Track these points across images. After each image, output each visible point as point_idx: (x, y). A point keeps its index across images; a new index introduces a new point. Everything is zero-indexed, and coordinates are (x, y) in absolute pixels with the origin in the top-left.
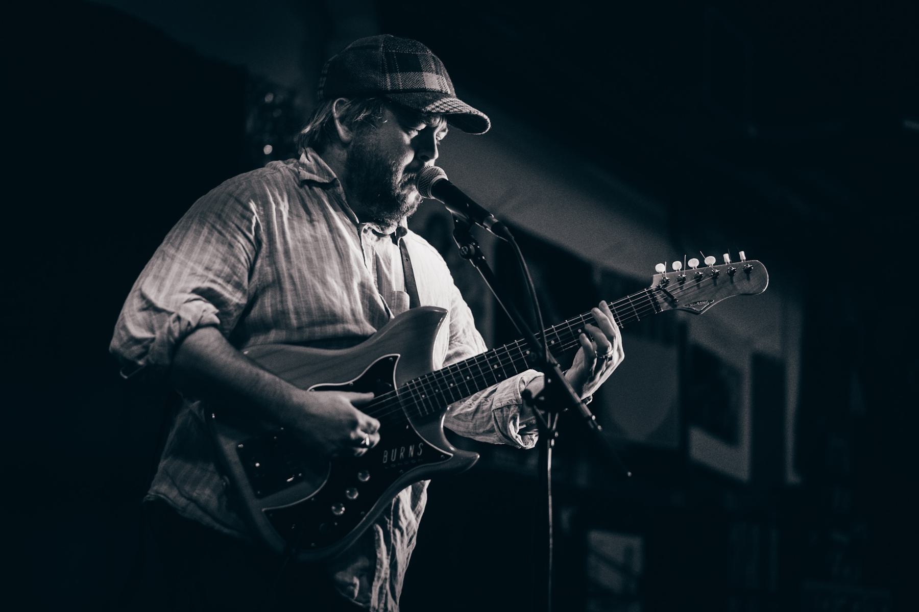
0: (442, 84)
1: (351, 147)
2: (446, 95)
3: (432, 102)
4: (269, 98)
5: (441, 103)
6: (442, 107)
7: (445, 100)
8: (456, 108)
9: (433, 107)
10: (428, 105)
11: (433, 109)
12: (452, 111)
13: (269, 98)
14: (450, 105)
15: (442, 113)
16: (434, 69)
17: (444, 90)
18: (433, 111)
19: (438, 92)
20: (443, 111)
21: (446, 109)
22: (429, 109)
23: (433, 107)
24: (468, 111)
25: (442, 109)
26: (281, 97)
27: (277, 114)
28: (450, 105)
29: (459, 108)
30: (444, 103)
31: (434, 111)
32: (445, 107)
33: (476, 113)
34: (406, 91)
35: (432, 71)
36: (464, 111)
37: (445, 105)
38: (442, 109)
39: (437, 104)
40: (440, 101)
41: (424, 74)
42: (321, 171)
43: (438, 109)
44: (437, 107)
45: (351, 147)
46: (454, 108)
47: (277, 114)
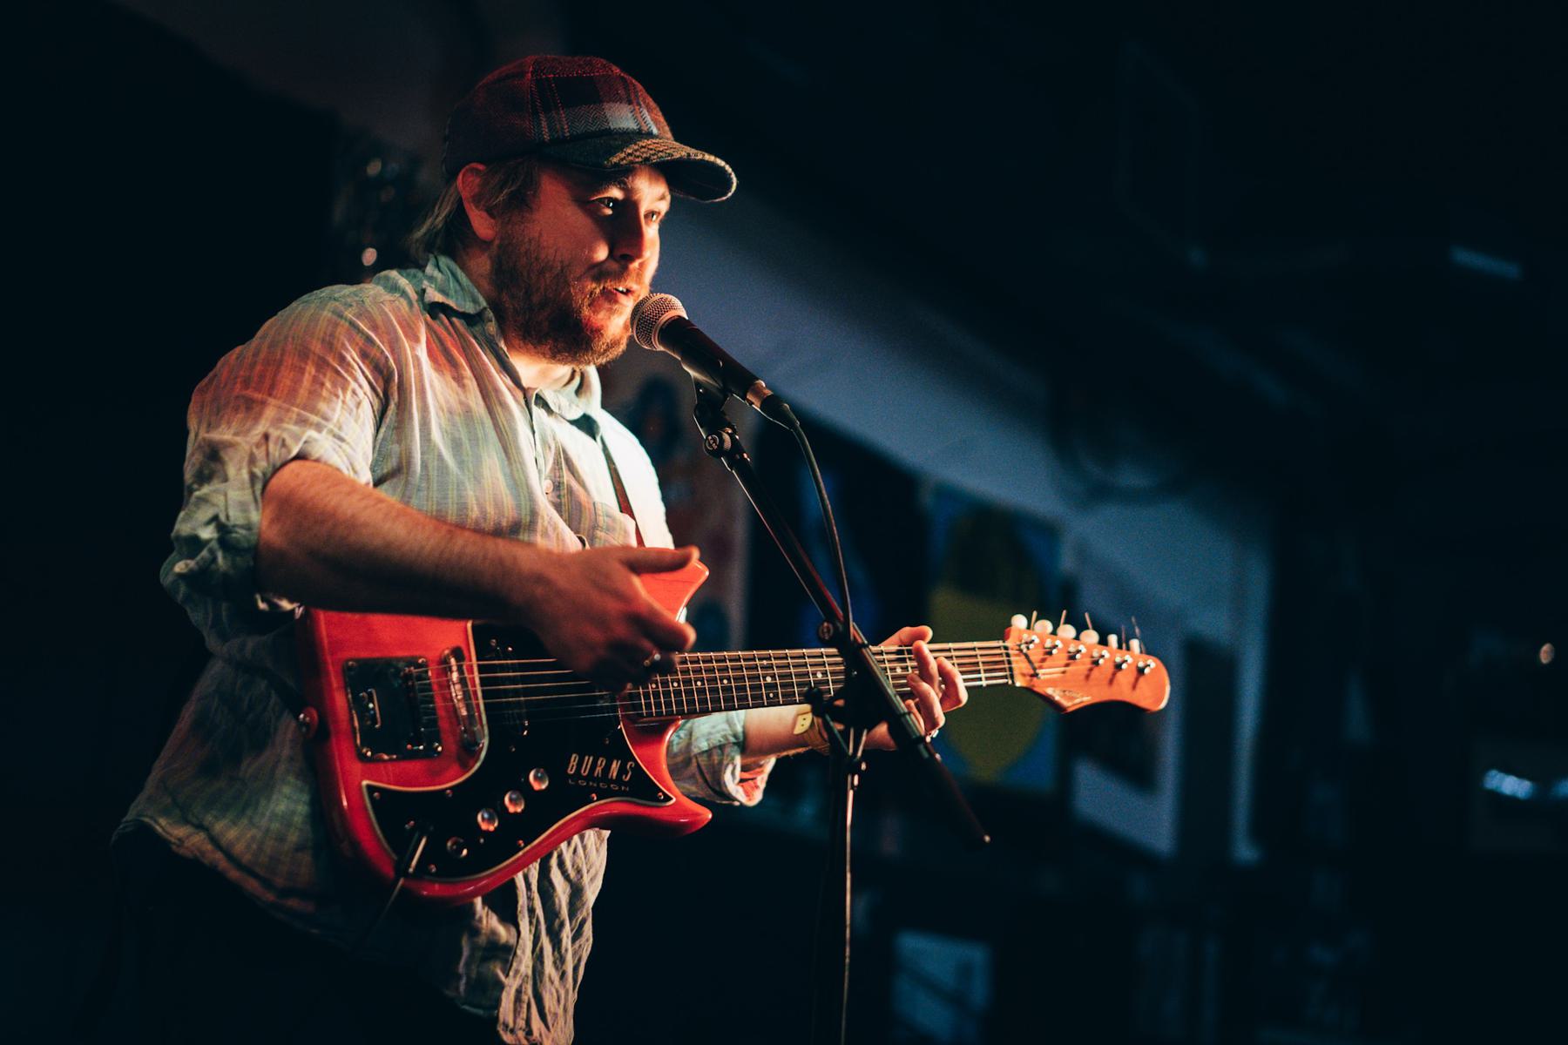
1: (494, 247)
4: (374, 168)
5: (636, 147)
6: (638, 153)
8: (662, 151)
9: (623, 155)
10: (613, 154)
11: (622, 159)
12: (655, 157)
13: (374, 168)
14: (651, 149)
18: (622, 163)
21: (645, 155)
22: (615, 160)
23: (623, 155)
24: (683, 153)
25: (638, 157)
26: (394, 166)
27: (387, 195)
28: (651, 149)
29: (668, 151)
30: (643, 147)
32: (643, 153)
33: (700, 157)
34: (575, 138)
36: (677, 156)
37: (643, 150)
38: (638, 157)
39: (630, 151)
40: (635, 144)
41: (606, 106)
42: (461, 293)
43: (630, 158)
45: (494, 247)
46: (659, 151)
47: (387, 195)
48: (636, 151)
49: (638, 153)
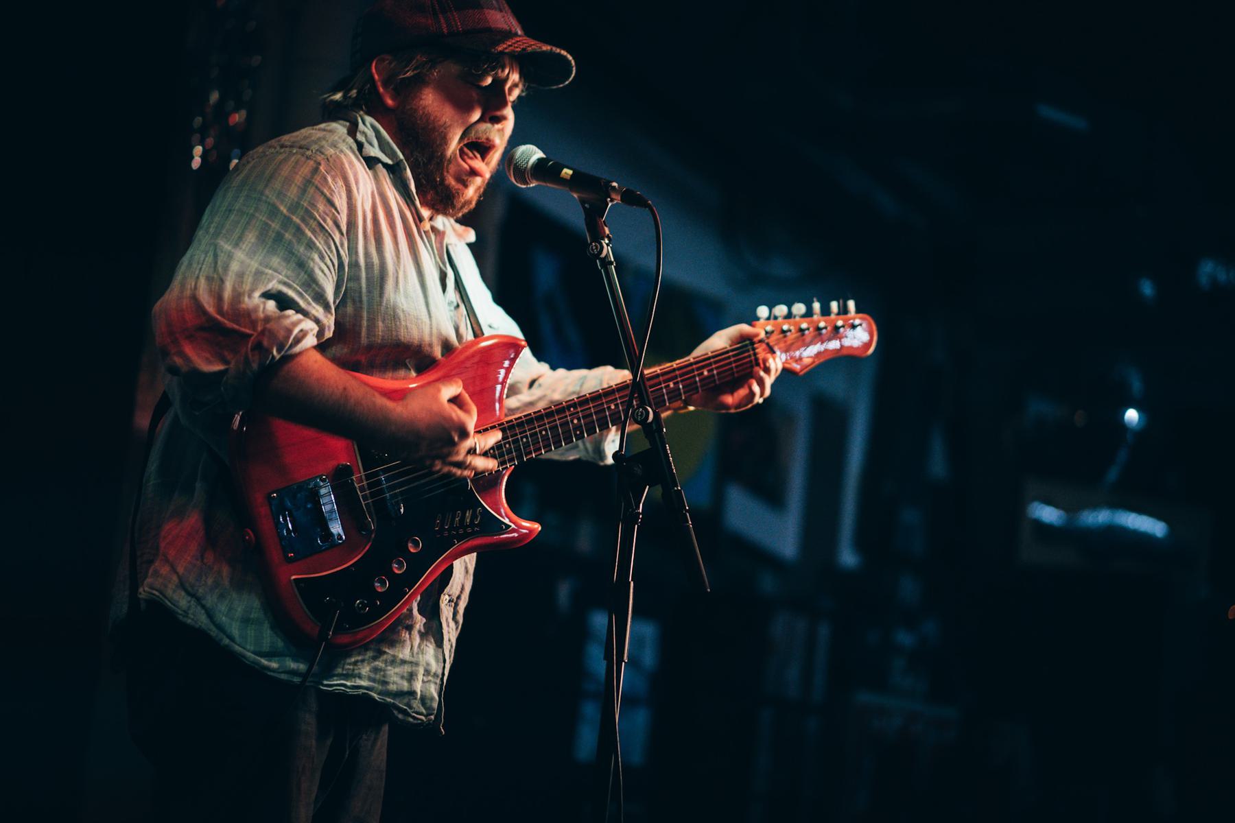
0: (509, 23)
2: (516, 34)
3: (502, 41)
5: (513, 41)
6: (516, 45)
7: (518, 39)
9: (505, 46)
10: (498, 45)
11: (506, 48)
12: (530, 48)
15: (517, 51)
16: (497, 6)
17: (513, 30)
19: (506, 30)
20: (519, 49)
21: (522, 47)
22: (500, 49)
23: (505, 46)
30: (518, 41)
31: (507, 51)
35: (495, 9)
44: (510, 46)
48: (514, 43)
49: (516, 45)
